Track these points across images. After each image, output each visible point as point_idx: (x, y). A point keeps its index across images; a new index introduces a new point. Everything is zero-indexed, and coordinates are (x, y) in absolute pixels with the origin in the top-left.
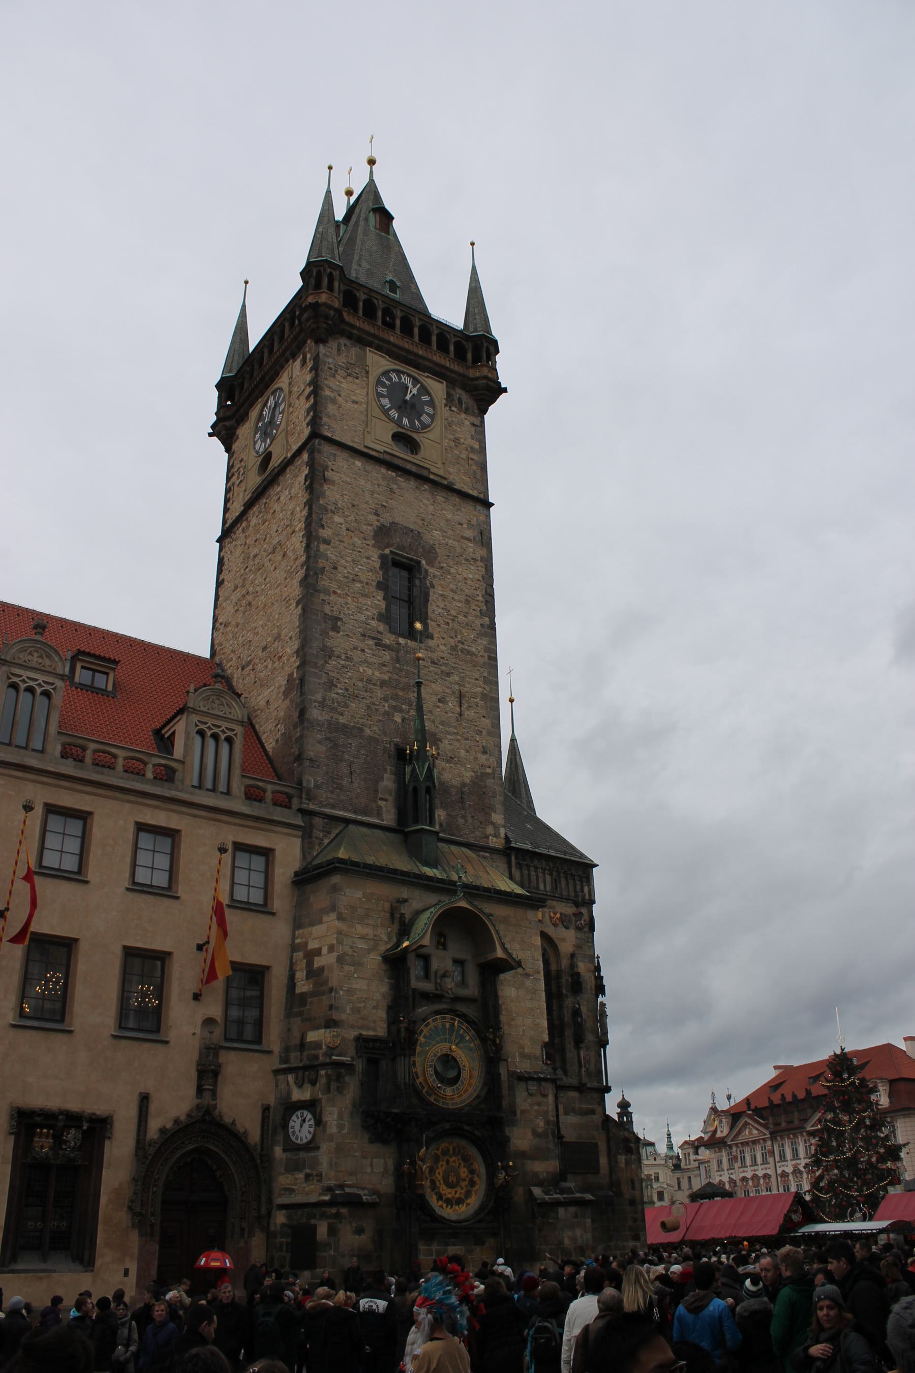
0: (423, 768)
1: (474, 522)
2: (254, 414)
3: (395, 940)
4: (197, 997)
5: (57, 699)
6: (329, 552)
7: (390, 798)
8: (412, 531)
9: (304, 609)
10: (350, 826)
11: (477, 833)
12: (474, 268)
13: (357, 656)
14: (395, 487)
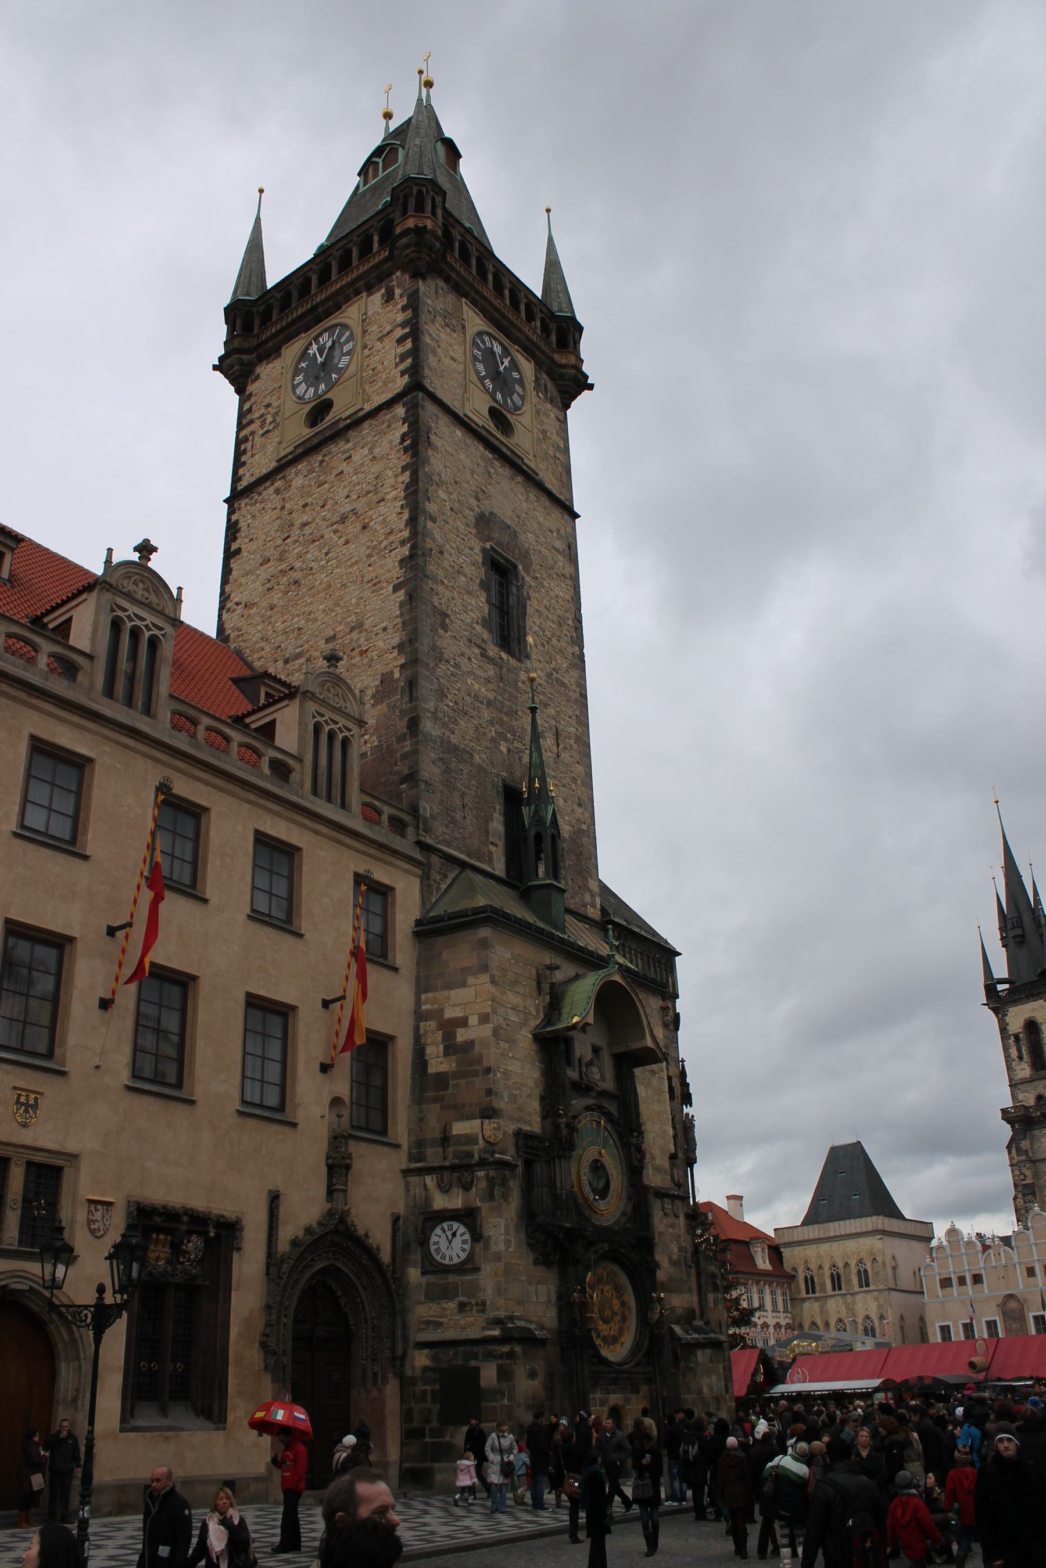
1: (562, 532)
2: (291, 352)
4: (325, 1068)
6: (437, 535)
7: (501, 843)
8: (509, 527)
9: (411, 597)
11: (577, 900)
13: (463, 662)
14: (492, 471)
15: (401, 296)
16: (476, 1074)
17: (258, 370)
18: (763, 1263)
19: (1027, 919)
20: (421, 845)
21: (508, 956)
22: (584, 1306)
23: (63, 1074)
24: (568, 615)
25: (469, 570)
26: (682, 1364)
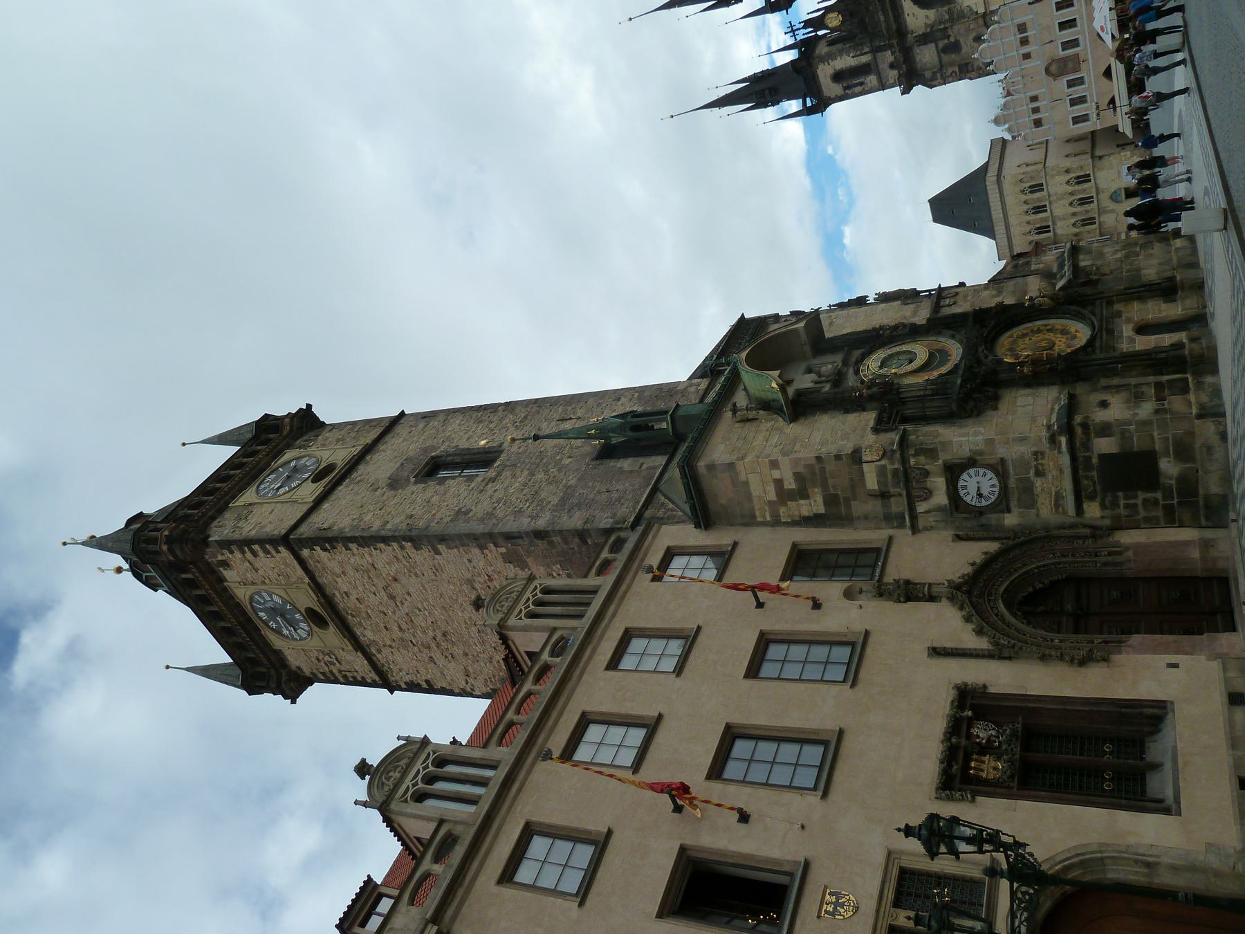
4: (817, 605)
7: (641, 460)
9: (443, 539)
10: (662, 486)
12: (203, 442)
13: (498, 495)
16: (823, 470)
17: (294, 668)
19: (758, 87)
20: (633, 526)
21: (722, 447)
22: (1035, 362)
23: (807, 864)
25: (428, 494)
26: (1095, 277)
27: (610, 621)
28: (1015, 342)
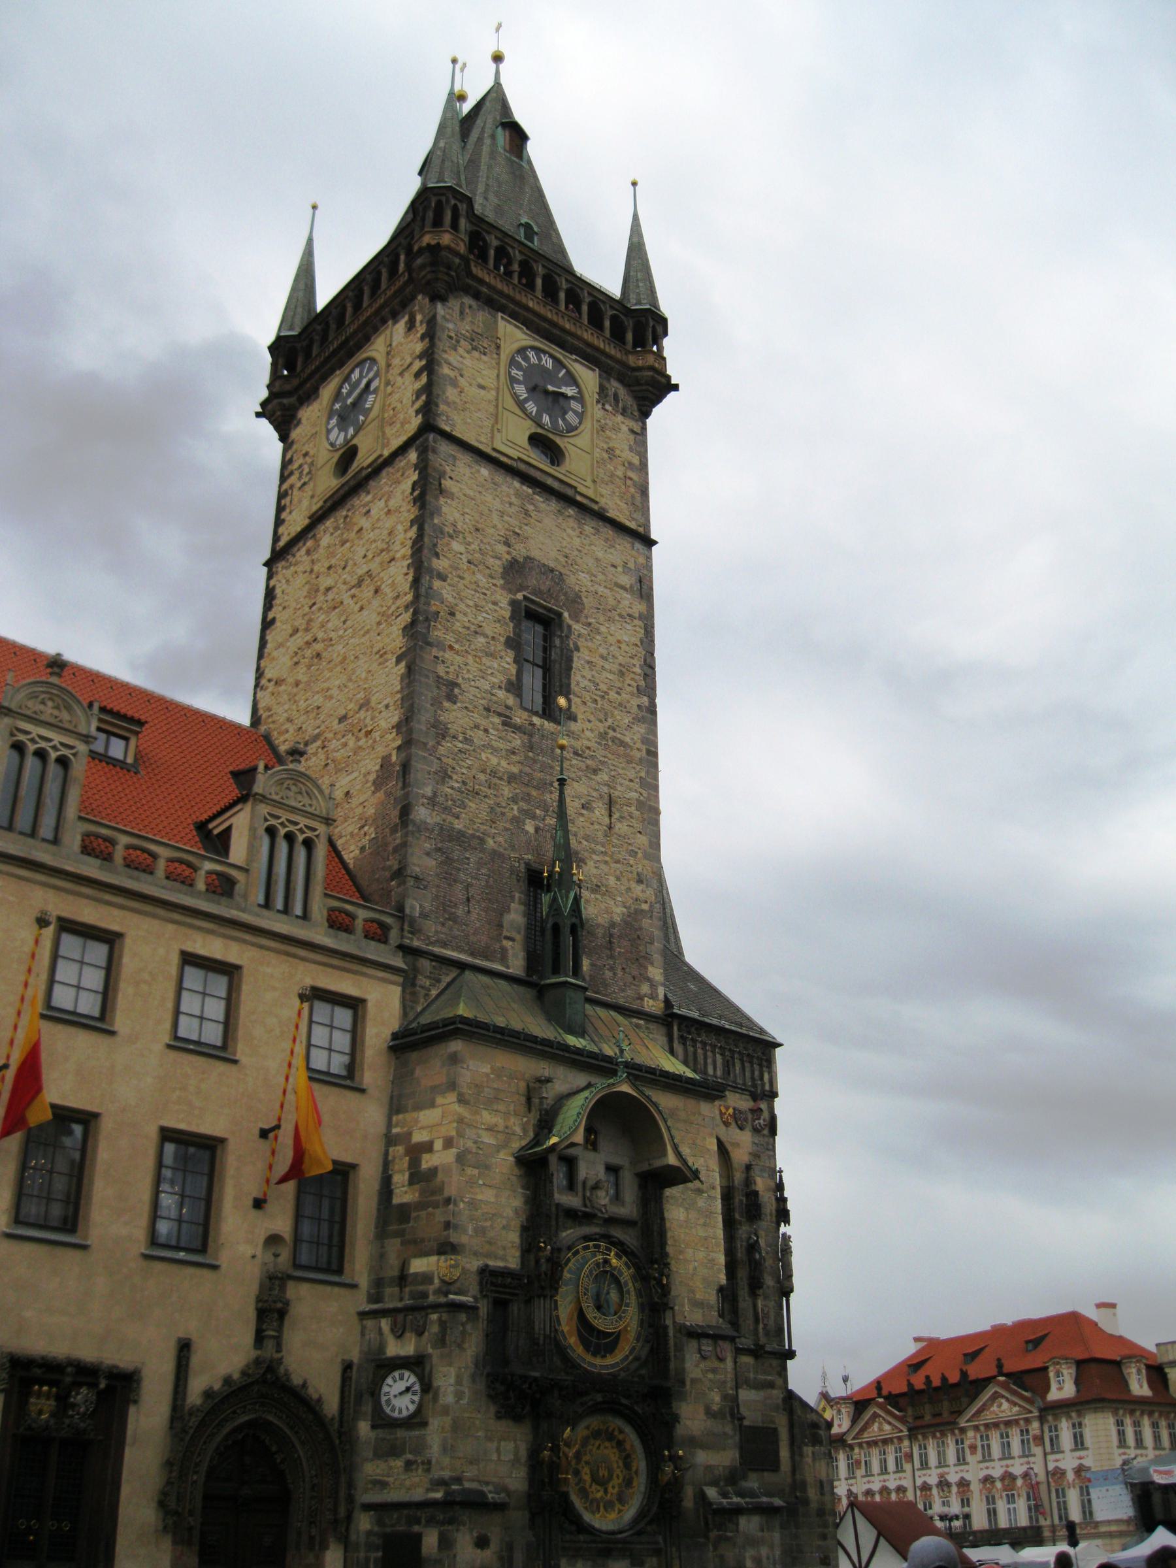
0: (567, 898)
1: (631, 565)
2: (327, 392)
3: (531, 1135)
4: (258, 1204)
5: (79, 767)
7: (519, 937)
8: (552, 571)
9: (410, 669)
10: (468, 974)
11: (629, 992)
12: (636, 218)
13: (478, 737)
14: (531, 508)
15: (421, 322)
16: (436, 1206)
18: (1139, 1387)
21: (486, 1069)
24: (635, 661)
26: (713, 1534)
27: (253, 944)
28: (610, 1437)
